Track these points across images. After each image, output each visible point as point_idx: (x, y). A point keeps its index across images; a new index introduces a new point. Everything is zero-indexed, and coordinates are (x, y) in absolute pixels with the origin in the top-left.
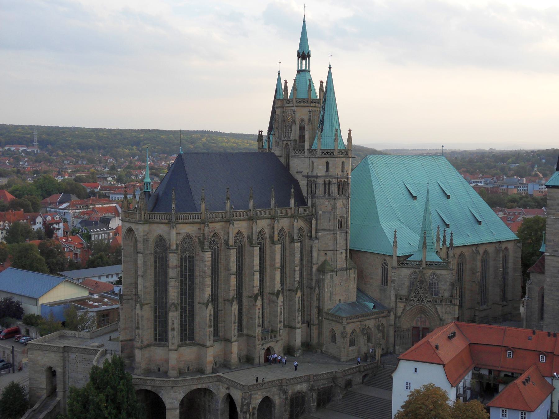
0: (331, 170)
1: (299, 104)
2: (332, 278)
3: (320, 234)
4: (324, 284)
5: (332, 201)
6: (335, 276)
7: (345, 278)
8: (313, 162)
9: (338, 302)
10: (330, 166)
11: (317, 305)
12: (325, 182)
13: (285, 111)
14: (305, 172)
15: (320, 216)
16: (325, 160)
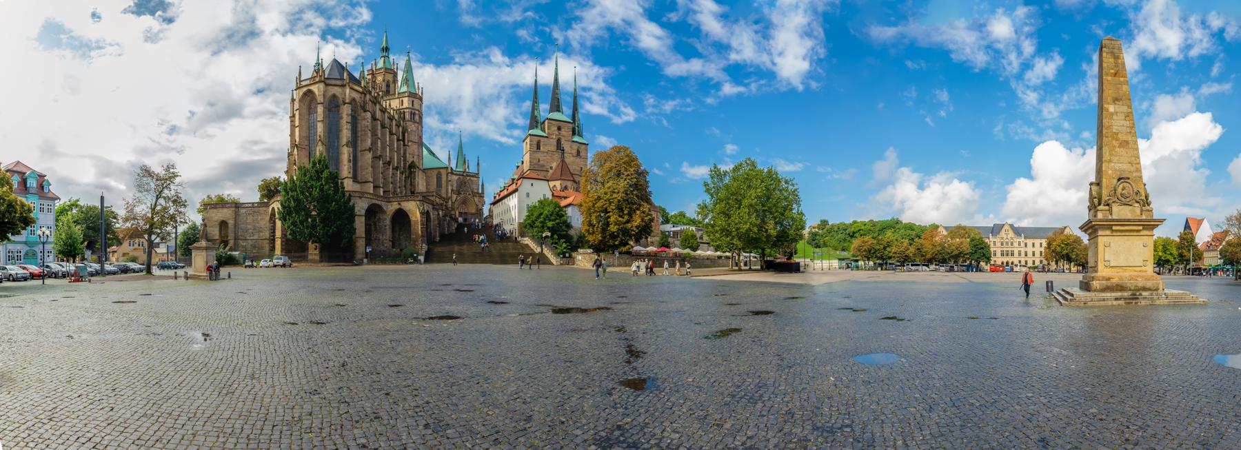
4: (415, 175)
5: (416, 125)
8: (402, 101)
10: (414, 103)
16: (411, 99)
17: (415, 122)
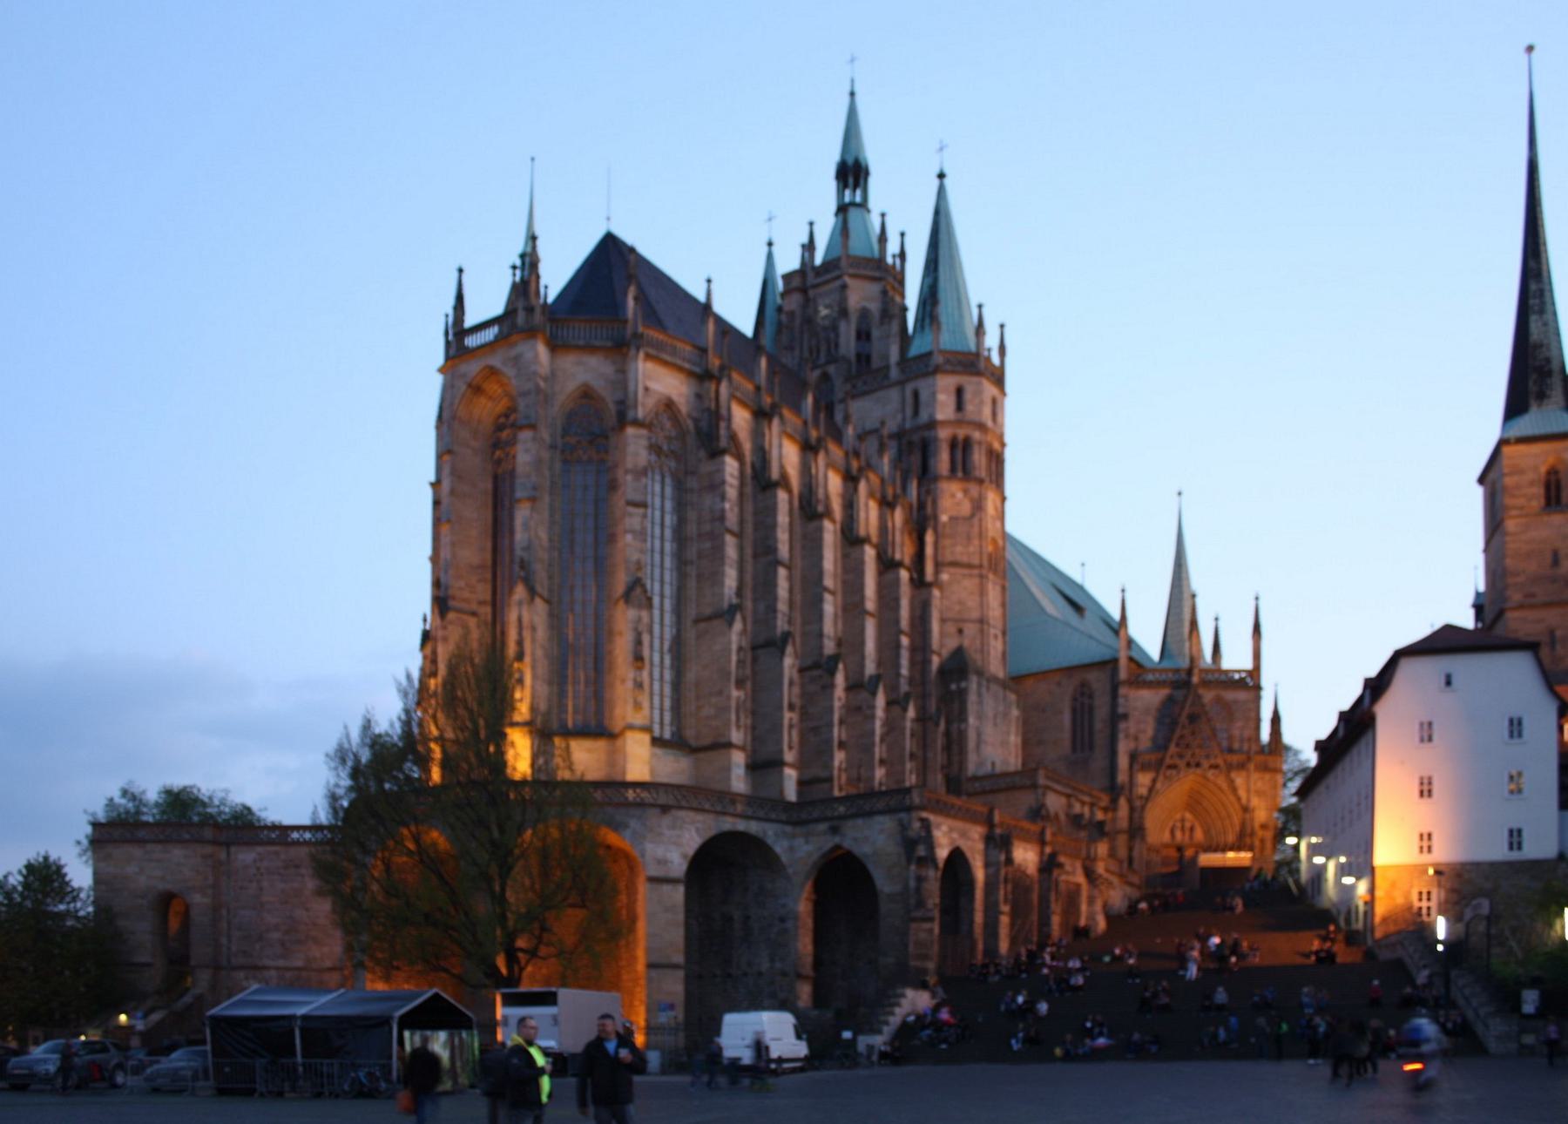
0: (969, 408)
2: (980, 695)
3: (945, 577)
5: (974, 490)
6: (984, 690)
8: (916, 395)
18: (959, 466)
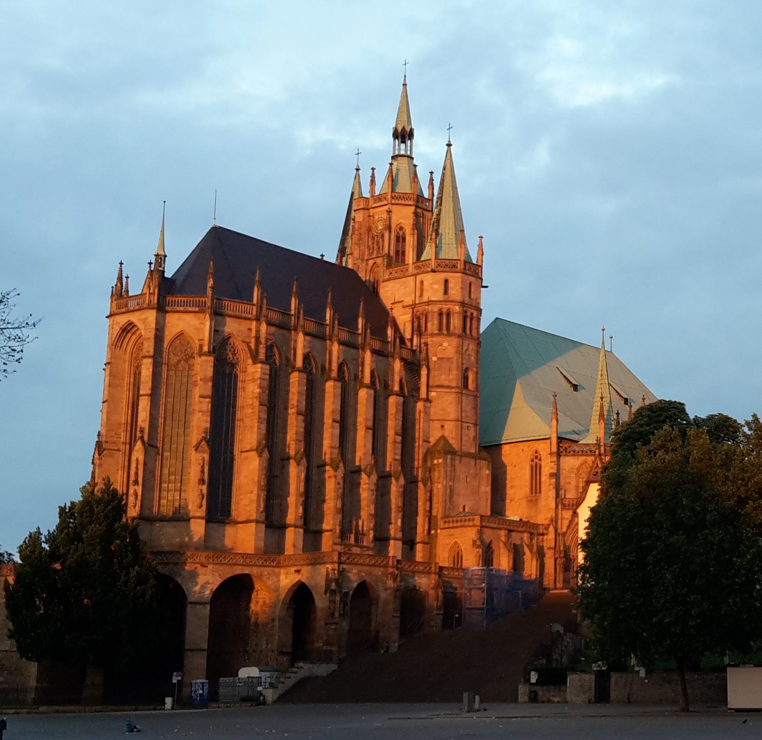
1: (397, 202)
3: (433, 394)
6: (457, 462)
7: (472, 471)
8: (422, 282)
9: (461, 510)
10: (451, 285)
11: (428, 509)
12: (441, 309)
13: (371, 214)
14: (409, 300)
15: (435, 364)
16: (442, 276)
17: (449, 334)
18: (444, 328)
